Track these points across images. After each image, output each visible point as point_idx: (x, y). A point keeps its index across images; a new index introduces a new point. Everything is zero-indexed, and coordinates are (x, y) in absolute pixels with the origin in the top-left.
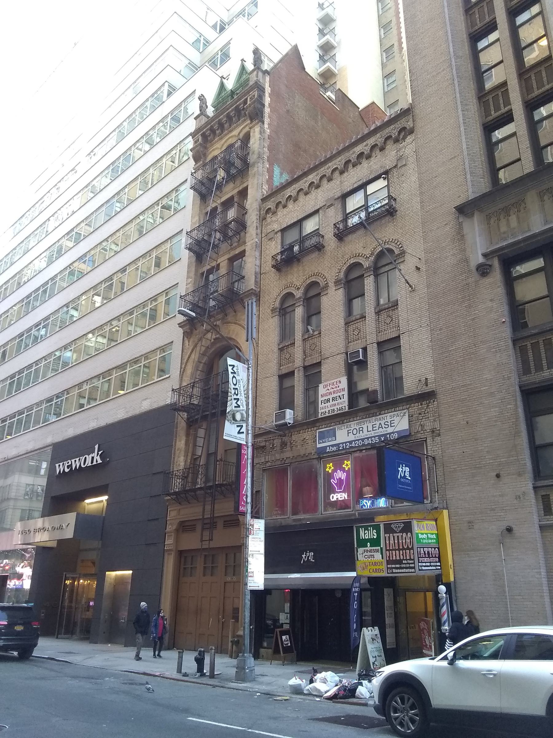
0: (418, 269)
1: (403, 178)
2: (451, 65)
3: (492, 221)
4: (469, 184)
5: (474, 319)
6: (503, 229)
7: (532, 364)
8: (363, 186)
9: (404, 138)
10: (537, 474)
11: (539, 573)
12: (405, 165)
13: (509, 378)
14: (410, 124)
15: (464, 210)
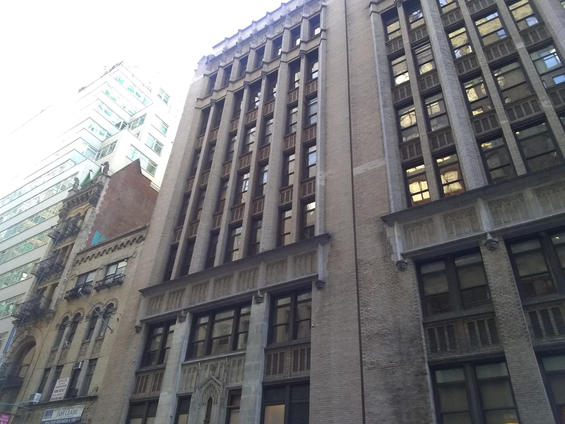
8: (117, 263)
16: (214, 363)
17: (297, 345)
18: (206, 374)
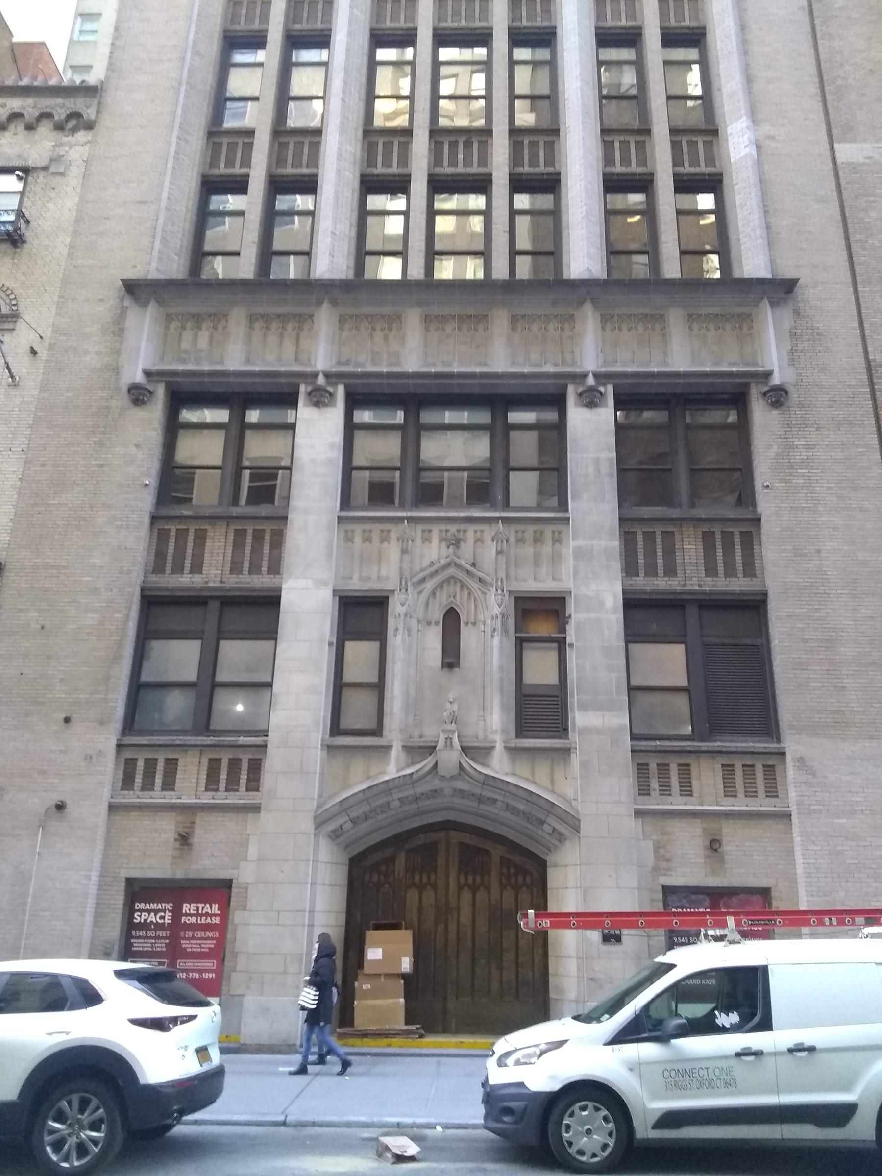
0: (34, 352)
1: (52, 194)
2: (183, 59)
3: (173, 326)
4: (155, 253)
5: (102, 466)
6: (185, 345)
7: (170, 559)
9: (74, 130)
10: (129, 725)
11: (88, 877)
12: (62, 174)
13: (129, 572)
14: (90, 113)
15: (135, 290)
16: (453, 528)
17: (714, 520)
18: (432, 551)
